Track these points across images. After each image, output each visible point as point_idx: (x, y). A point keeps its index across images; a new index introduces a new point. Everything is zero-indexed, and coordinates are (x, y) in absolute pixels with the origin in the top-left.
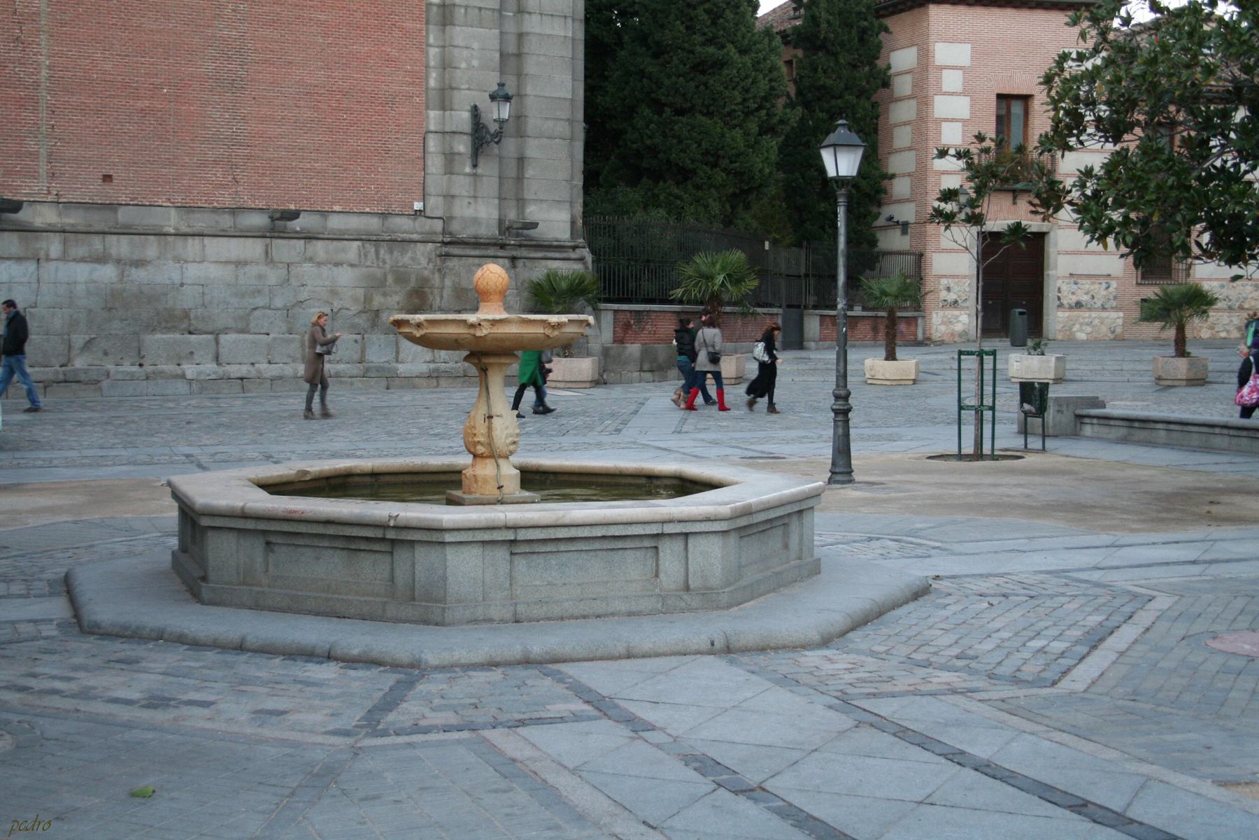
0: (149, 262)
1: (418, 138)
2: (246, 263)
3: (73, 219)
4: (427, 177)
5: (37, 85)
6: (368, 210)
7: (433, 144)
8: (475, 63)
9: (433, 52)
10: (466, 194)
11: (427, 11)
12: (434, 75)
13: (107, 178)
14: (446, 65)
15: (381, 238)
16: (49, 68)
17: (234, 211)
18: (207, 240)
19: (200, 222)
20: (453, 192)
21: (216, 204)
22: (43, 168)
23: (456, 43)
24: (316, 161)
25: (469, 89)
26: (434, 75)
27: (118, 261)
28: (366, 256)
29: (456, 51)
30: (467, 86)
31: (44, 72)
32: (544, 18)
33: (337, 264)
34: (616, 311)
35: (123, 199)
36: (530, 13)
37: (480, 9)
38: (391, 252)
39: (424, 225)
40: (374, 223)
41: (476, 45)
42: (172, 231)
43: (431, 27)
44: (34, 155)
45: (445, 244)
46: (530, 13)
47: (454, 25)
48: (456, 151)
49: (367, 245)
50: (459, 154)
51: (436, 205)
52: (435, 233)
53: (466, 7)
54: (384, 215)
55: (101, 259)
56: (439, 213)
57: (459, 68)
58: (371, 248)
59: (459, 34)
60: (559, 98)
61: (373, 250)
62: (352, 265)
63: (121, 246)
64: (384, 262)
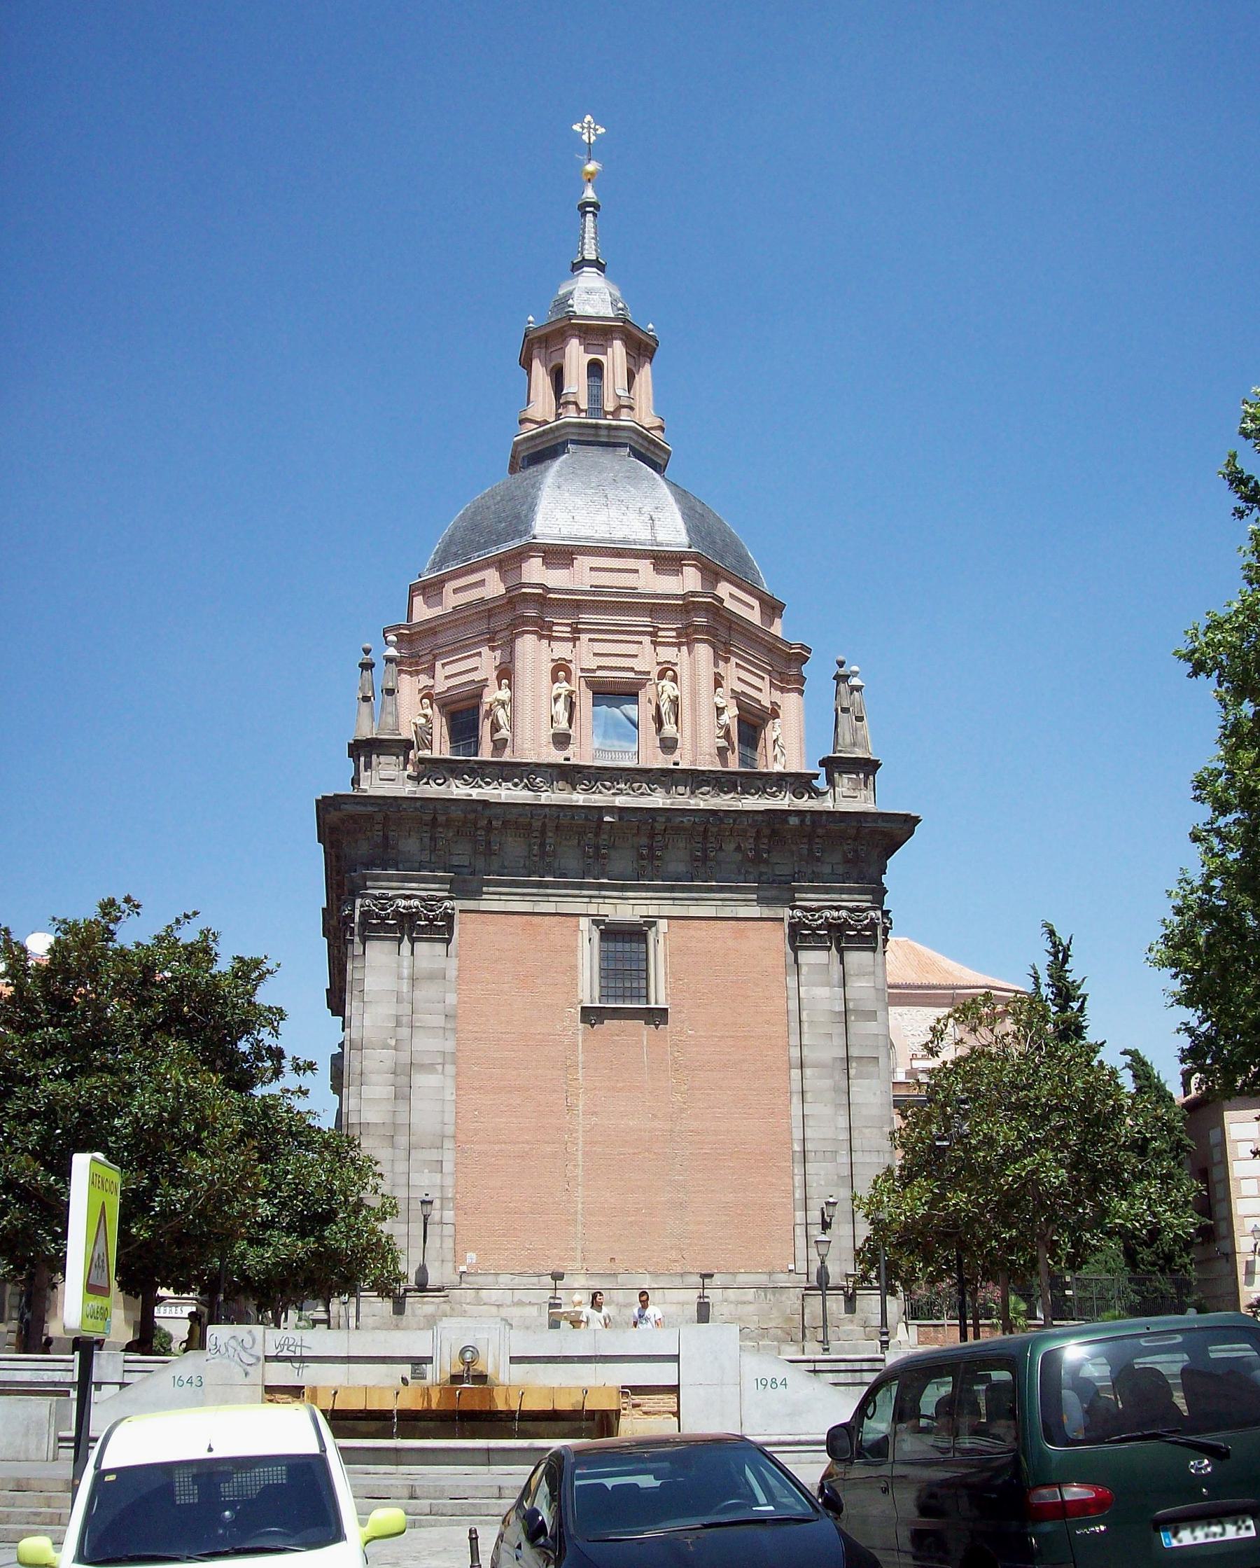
2: (688, 1304)
5: (576, 1212)
16: (582, 1203)
17: (682, 1275)
22: (579, 1255)
24: (729, 1244)
27: (617, 1305)
31: (580, 1206)
34: (918, 1326)
35: (621, 1271)
38: (774, 1295)
40: (763, 1279)
41: (822, 1173)
43: (795, 1165)
49: (759, 1290)
53: (815, 1152)
54: (770, 1274)
58: (761, 1293)
64: (770, 1300)
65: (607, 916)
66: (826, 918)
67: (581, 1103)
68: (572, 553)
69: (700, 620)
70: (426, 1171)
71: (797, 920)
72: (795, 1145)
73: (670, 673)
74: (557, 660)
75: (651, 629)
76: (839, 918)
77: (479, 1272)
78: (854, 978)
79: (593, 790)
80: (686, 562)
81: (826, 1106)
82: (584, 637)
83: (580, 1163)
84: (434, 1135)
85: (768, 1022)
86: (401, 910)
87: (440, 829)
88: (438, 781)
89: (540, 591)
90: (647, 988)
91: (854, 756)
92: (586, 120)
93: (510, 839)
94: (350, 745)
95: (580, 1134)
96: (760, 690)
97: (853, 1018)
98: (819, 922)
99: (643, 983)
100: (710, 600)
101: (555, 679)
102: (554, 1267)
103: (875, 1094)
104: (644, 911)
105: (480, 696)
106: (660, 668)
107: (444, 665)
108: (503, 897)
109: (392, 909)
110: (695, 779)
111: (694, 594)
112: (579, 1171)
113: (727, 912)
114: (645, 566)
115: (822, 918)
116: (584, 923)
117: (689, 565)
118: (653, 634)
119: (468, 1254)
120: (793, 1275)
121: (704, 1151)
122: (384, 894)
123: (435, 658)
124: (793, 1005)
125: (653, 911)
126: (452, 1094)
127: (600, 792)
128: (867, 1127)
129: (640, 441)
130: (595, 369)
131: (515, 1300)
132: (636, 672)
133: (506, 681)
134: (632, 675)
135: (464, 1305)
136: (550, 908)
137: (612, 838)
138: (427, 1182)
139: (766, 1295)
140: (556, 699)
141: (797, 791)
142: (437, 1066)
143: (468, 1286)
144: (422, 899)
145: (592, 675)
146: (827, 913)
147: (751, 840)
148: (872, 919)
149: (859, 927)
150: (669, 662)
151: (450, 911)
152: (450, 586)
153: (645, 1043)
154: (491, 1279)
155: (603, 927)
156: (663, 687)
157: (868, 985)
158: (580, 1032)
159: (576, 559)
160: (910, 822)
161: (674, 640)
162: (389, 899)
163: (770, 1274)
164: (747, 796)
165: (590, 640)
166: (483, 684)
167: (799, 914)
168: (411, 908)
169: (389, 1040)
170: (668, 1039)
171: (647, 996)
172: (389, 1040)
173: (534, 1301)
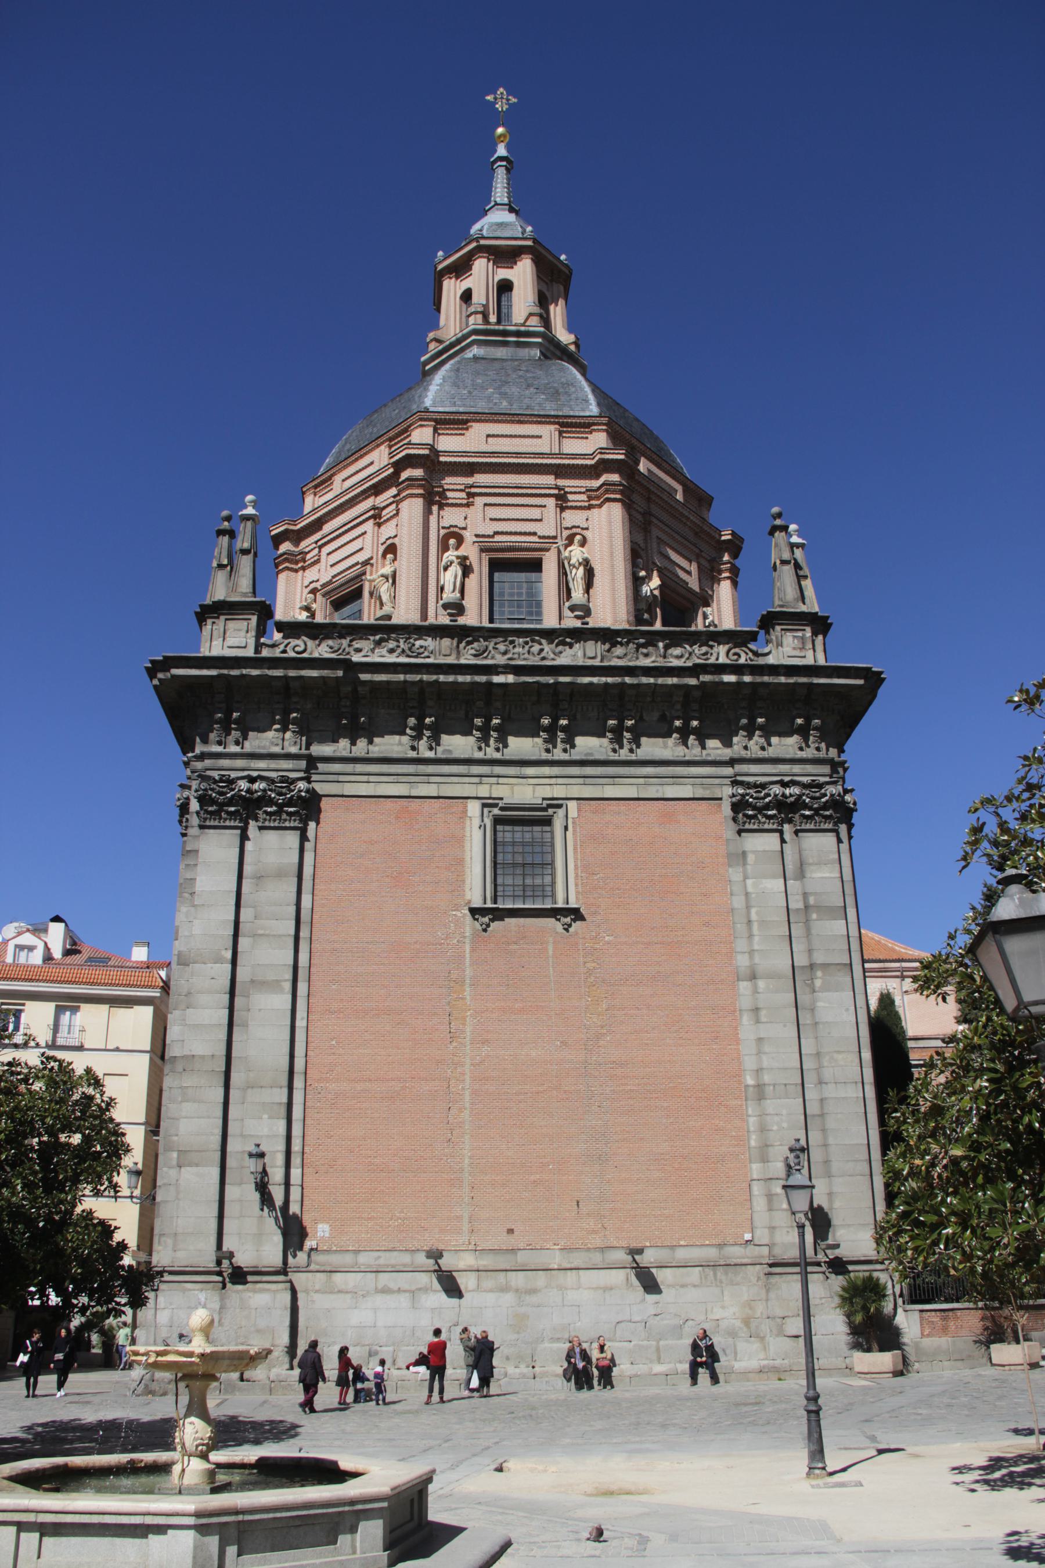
0: (540, 1291)
1: (745, 1185)
3: (485, 1262)
4: (755, 1215)
5: (462, 1170)
6: (707, 1242)
7: (756, 1188)
8: (785, 1125)
9: (752, 1120)
10: (785, 1225)
11: (746, 1091)
12: (754, 1137)
13: (511, 1231)
14: (763, 1129)
15: (718, 1263)
16: (470, 1158)
17: (602, 1250)
18: (581, 1272)
19: (577, 1260)
20: (773, 1225)
21: (589, 1245)
22: (466, 1227)
23: (768, 1112)
25: (781, 1145)
26: (754, 1137)
27: (517, 1291)
28: (706, 1278)
29: (768, 1118)
30: (778, 1143)
31: (467, 1161)
32: (838, 1085)
33: (683, 1286)
34: (921, 1311)
35: (521, 1246)
36: (826, 1083)
37: (785, 1085)
38: (726, 1274)
39: (752, 1251)
40: (712, 1253)
41: (784, 1112)
42: (556, 1267)
43: (749, 1102)
44: (459, 1218)
45: (771, 1265)
46: (826, 1083)
47: (766, 1099)
48: (773, 1192)
49: (707, 1269)
50: (777, 1194)
51: (762, 1236)
52: (763, 1257)
53: (774, 1085)
54: (720, 1246)
55: (504, 1289)
56: (765, 1241)
57: (772, 1130)
59: (770, 1105)
60: (857, 1144)
61: (712, 1273)
62: (695, 1286)
63: (518, 1279)
65: (502, 799)
66: (776, 795)
67: (468, 1029)
68: (466, 422)
69: (615, 478)
70: (265, 1116)
71: (738, 798)
72: (748, 1077)
73: (578, 537)
74: (448, 528)
75: (556, 492)
76: (791, 795)
77: (335, 1248)
78: (812, 868)
79: (485, 655)
80: (596, 427)
81: (785, 1026)
82: (479, 501)
83: (467, 1105)
84: (277, 1070)
85: (707, 924)
86: (244, 794)
87: (295, 699)
88: (297, 649)
89: (427, 452)
90: (553, 884)
91: (798, 610)
92: (499, 93)
93: (383, 711)
94: (196, 613)
95: (467, 1068)
96: (689, 573)
97: (814, 916)
98: (767, 800)
99: (548, 880)
100: (622, 457)
101: (444, 547)
102: (431, 1241)
103: (847, 1010)
104: (548, 792)
105: (364, 573)
106: (566, 533)
107: (328, 554)
108: (372, 778)
109: (233, 793)
110: (608, 636)
111: (602, 450)
112: (466, 1115)
113: (652, 792)
114: (548, 431)
115: (768, 795)
116: (474, 808)
117: (599, 430)
118: (558, 497)
119: (320, 1226)
120: (751, 1247)
121: (629, 1087)
122: (224, 776)
123: (320, 547)
124: (738, 902)
125: (559, 792)
126: (302, 1019)
127: (493, 658)
128: (839, 1052)
129: (552, 348)
130: (505, 287)
131: (380, 1287)
132: (540, 537)
133: (392, 556)
134: (535, 539)
135: (312, 1294)
136: (431, 790)
137: (507, 707)
138: (265, 1131)
139: (715, 1275)
140: (446, 569)
141: (733, 651)
142: (283, 984)
143: (317, 1267)
144: (270, 781)
145: (491, 540)
146: (776, 789)
147: (678, 707)
148: (832, 795)
149: (815, 806)
150: (578, 527)
151: (303, 794)
152: (338, 478)
153: (551, 952)
154: (348, 1259)
155: (496, 811)
156: (571, 551)
157: (832, 875)
158: (467, 941)
159: (471, 426)
160: (874, 680)
161: (586, 504)
162: (231, 782)
163: (720, 1246)
164: (671, 660)
165: (486, 505)
166: (367, 562)
167: (741, 791)
168: (256, 791)
169: (223, 952)
170: (580, 947)
171: (553, 896)
172: (223, 952)
173: (407, 1287)
